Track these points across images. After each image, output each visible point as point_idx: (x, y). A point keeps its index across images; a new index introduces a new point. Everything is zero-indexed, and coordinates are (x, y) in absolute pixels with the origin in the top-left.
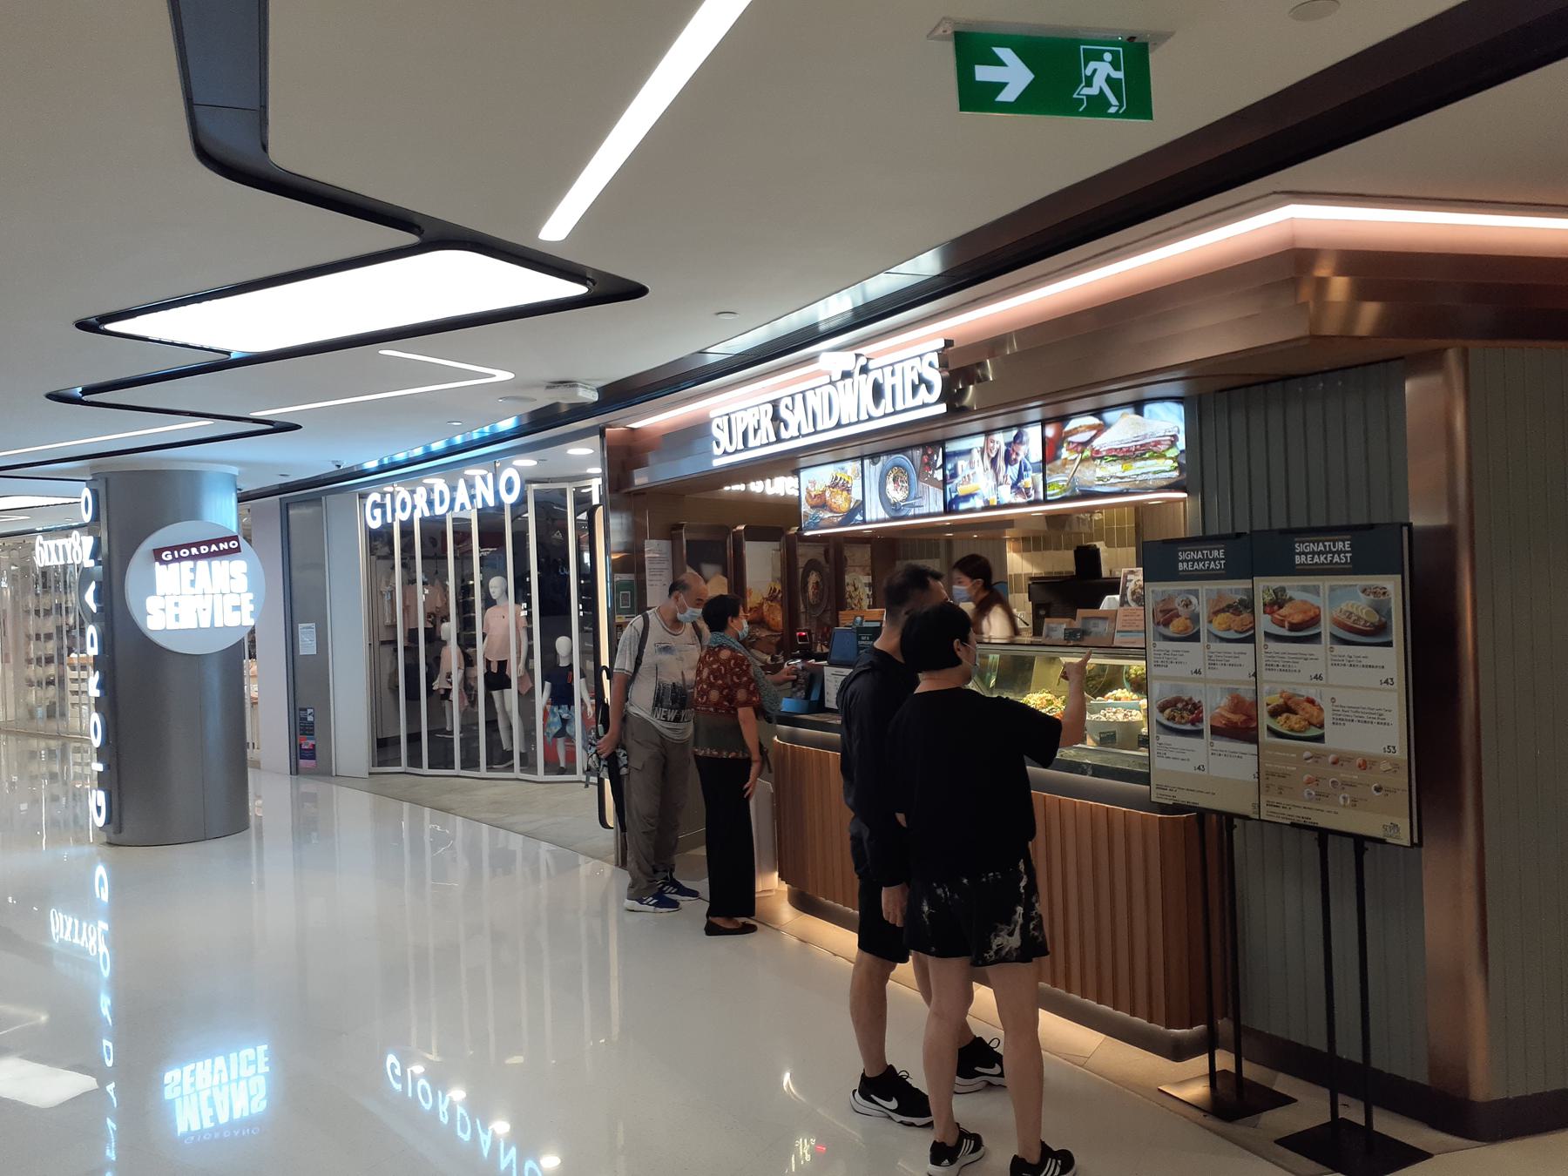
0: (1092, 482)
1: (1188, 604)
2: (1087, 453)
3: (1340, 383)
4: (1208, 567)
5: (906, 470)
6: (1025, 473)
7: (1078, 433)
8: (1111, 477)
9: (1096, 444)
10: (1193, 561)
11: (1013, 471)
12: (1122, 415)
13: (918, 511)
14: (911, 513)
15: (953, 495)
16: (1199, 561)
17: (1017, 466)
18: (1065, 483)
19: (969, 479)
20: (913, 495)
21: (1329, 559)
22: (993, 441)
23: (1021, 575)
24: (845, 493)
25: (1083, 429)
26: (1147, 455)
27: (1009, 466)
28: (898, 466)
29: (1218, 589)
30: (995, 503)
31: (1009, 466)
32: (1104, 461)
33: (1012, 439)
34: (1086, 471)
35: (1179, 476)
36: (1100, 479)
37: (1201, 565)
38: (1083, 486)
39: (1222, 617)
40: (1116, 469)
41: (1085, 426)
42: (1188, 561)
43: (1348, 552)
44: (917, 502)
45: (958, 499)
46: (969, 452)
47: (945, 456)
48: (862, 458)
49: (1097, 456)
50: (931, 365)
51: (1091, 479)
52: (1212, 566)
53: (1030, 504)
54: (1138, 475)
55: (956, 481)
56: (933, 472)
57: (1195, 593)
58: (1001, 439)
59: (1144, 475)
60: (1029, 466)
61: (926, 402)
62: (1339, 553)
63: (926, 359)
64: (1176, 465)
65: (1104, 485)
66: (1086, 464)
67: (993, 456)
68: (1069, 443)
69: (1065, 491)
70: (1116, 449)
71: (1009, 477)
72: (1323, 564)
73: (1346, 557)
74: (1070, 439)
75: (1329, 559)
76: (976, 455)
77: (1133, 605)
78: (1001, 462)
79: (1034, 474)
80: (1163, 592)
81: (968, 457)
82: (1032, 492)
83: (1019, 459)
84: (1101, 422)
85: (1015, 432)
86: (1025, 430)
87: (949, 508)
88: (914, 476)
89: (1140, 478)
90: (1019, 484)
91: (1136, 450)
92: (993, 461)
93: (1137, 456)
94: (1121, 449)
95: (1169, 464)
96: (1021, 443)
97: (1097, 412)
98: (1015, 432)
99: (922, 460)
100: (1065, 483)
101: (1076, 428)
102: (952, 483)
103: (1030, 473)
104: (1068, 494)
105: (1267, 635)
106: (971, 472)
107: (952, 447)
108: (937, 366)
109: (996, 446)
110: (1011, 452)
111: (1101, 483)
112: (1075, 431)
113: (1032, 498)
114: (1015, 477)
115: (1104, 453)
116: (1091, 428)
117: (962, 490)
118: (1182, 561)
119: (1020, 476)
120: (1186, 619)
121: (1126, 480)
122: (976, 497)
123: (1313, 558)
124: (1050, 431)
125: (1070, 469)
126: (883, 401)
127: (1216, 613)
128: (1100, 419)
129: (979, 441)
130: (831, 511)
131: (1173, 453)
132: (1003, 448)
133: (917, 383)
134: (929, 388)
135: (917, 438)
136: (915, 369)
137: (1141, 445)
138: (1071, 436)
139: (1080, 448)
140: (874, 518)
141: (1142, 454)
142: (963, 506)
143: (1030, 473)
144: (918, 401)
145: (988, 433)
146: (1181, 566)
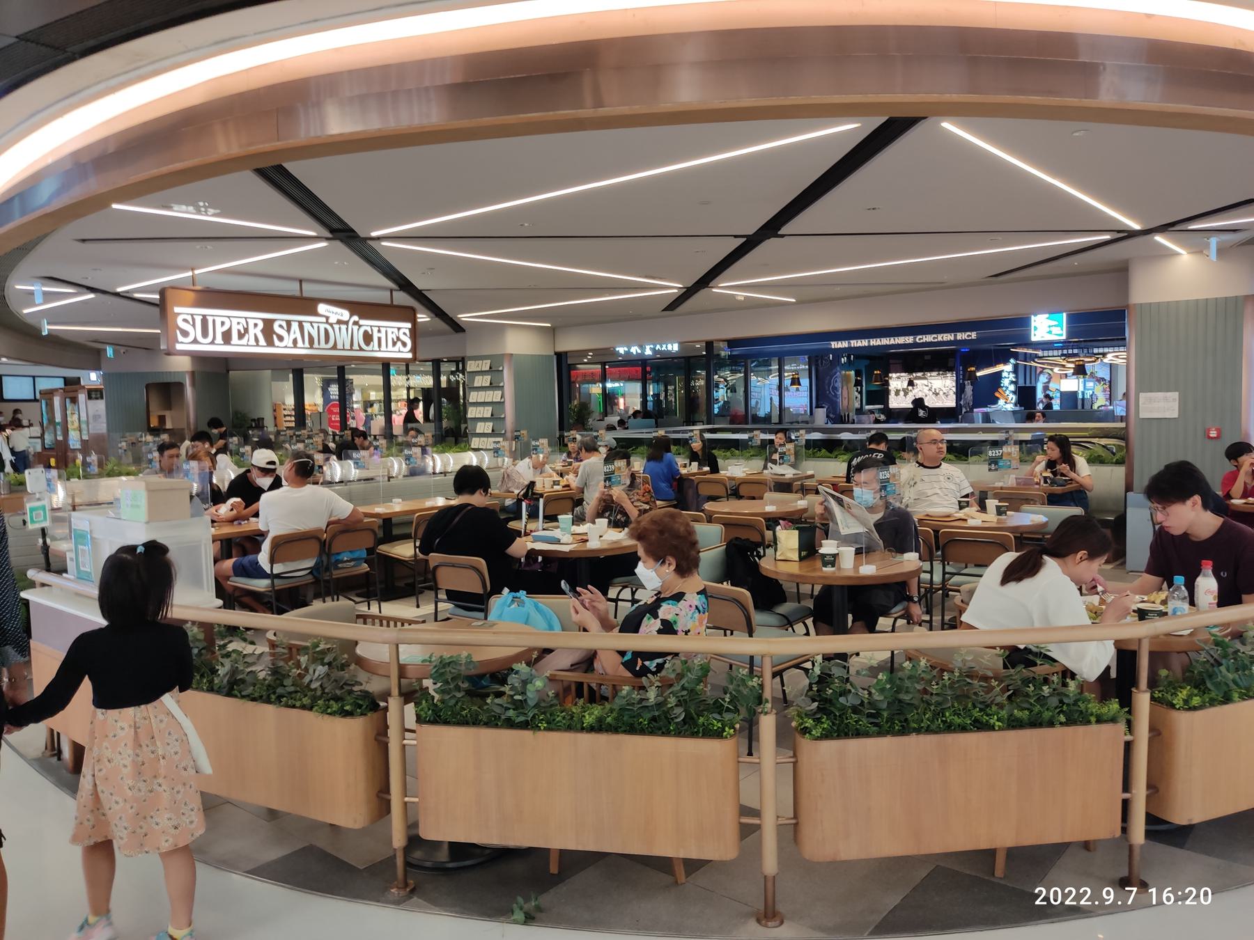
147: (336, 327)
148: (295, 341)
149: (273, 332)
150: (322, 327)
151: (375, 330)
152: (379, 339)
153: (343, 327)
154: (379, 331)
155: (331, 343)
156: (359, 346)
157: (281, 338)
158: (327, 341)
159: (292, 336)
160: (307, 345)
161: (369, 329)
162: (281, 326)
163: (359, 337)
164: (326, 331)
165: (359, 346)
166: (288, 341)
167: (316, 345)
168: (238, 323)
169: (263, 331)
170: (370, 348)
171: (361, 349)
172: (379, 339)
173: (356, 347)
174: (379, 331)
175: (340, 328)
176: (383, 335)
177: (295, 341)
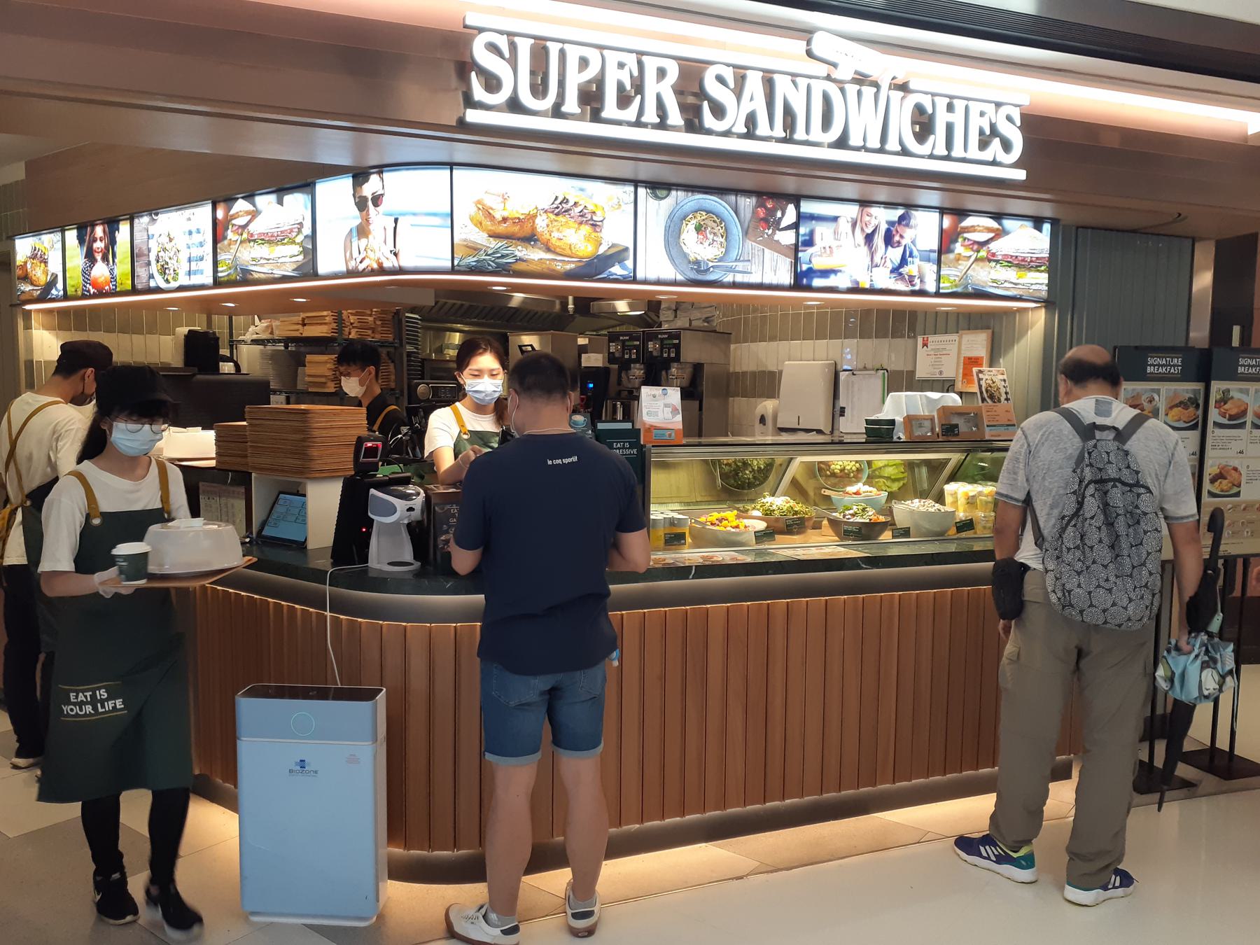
0: (986, 282)
1: (1151, 400)
2: (983, 253)
3: (1160, 245)
4: (1169, 371)
5: (722, 220)
6: (909, 259)
7: (974, 231)
8: (1005, 281)
9: (993, 246)
10: (1159, 365)
11: (895, 254)
12: (1022, 225)
13: (740, 278)
14: (729, 278)
15: (805, 267)
16: (1163, 366)
17: (900, 250)
18: (957, 279)
19: (831, 252)
20: (734, 255)
21: (1168, 370)
22: (869, 215)
23: (746, 372)
24: (586, 229)
25: (981, 228)
26: (1043, 268)
27: (890, 248)
28: (708, 212)
29: (1175, 389)
30: (867, 286)
31: (890, 248)
32: (999, 265)
33: (896, 219)
34: (981, 270)
35: (304, 259)
36: (994, 281)
37: (1164, 370)
38: (976, 285)
39: (1176, 410)
40: (1011, 274)
41: (983, 226)
42: (1154, 366)
43: (1180, 366)
44: (740, 266)
45: (811, 273)
46: (835, 219)
47: (800, 216)
48: (636, 183)
49: (991, 259)
50: (1009, 119)
51: (985, 279)
52: (1172, 371)
53: (914, 293)
54: (1032, 284)
55: (810, 250)
56: (774, 233)
57: (1158, 392)
58: (881, 217)
59: (1038, 286)
60: (915, 253)
61: (998, 159)
62: (1174, 366)
63: (1004, 111)
64: (301, 249)
65: (998, 287)
66: (981, 264)
67: (869, 231)
68: (965, 239)
69: (956, 286)
70: (1012, 256)
71: (888, 260)
72: (1164, 373)
73: (1178, 369)
74: (966, 235)
75: (1168, 370)
76: (844, 225)
77: (989, 400)
78: (879, 240)
79: (922, 263)
80: (1134, 390)
81: (832, 225)
82: (917, 281)
83: (904, 242)
84: (1000, 228)
85: (900, 212)
86: (913, 212)
87: (797, 286)
88: (737, 231)
89: (1034, 287)
90: (901, 270)
91: (1031, 261)
92: (869, 238)
93: (1032, 267)
94: (1017, 257)
95: (296, 249)
96: (907, 225)
97: (998, 216)
98: (900, 212)
99: (754, 212)
100: (957, 279)
101: (973, 226)
102: (805, 251)
103: (917, 261)
104: (959, 290)
105: (988, 426)
106: (834, 244)
107: (808, 207)
108: (1018, 123)
109: (874, 222)
110: (894, 233)
111: (995, 285)
112: (971, 229)
113: (917, 288)
114: (897, 260)
115: (1000, 258)
116: (990, 230)
117: (818, 264)
118: (1151, 365)
119: (904, 262)
120: (1149, 412)
121: (1020, 286)
122: (839, 274)
123: (1158, 369)
124: (947, 222)
125: (964, 265)
126: (932, 138)
127: (1171, 408)
128: (1000, 224)
129: (852, 210)
130: (548, 249)
131: (300, 239)
132: (884, 227)
133: (988, 132)
134: (1007, 146)
135: (748, 181)
136: (987, 117)
137: (1037, 258)
138: (968, 232)
139: (976, 247)
140: (652, 276)
141: (1037, 266)
142: (817, 282)
143: (917, 261)
144: (987, 155)
145: (864, 203)
146: (1149, 370)
147: (852, 89)
148: (751, 120)
149: (702, 94)
150: (818, 87)
151: (942, 103)
152: (950, 128)
153: (868, 91)
154: (950, 108)
155: (835, 133)
156: (901, 143)
157: (719, 111)
158: (827, 123)
159: (746, 107)
160: (779, 132)
161: (926, 102)
162: (720, 79)
163: (902, 126)
164: (827, 100)
165: (901, 143)
166: (735, 118)
167: (800, 134)
168: (982, 114)
169: (679, 91)
170: (925, 149)
171: (905, 152)
172: (950, 128)
173: (893, 145)
174: (950, 108)
175: (859, 93)
176: (957, 119)
177: (751, 120)
